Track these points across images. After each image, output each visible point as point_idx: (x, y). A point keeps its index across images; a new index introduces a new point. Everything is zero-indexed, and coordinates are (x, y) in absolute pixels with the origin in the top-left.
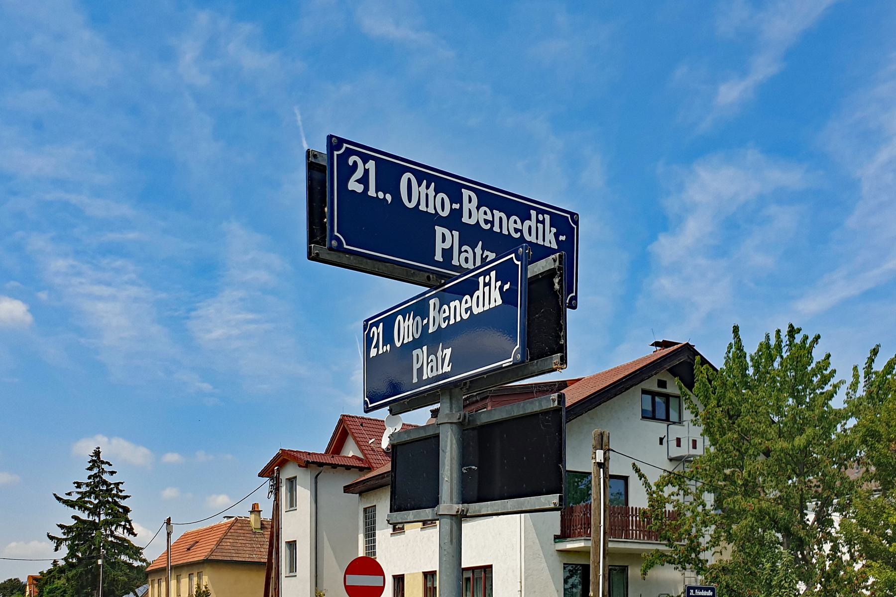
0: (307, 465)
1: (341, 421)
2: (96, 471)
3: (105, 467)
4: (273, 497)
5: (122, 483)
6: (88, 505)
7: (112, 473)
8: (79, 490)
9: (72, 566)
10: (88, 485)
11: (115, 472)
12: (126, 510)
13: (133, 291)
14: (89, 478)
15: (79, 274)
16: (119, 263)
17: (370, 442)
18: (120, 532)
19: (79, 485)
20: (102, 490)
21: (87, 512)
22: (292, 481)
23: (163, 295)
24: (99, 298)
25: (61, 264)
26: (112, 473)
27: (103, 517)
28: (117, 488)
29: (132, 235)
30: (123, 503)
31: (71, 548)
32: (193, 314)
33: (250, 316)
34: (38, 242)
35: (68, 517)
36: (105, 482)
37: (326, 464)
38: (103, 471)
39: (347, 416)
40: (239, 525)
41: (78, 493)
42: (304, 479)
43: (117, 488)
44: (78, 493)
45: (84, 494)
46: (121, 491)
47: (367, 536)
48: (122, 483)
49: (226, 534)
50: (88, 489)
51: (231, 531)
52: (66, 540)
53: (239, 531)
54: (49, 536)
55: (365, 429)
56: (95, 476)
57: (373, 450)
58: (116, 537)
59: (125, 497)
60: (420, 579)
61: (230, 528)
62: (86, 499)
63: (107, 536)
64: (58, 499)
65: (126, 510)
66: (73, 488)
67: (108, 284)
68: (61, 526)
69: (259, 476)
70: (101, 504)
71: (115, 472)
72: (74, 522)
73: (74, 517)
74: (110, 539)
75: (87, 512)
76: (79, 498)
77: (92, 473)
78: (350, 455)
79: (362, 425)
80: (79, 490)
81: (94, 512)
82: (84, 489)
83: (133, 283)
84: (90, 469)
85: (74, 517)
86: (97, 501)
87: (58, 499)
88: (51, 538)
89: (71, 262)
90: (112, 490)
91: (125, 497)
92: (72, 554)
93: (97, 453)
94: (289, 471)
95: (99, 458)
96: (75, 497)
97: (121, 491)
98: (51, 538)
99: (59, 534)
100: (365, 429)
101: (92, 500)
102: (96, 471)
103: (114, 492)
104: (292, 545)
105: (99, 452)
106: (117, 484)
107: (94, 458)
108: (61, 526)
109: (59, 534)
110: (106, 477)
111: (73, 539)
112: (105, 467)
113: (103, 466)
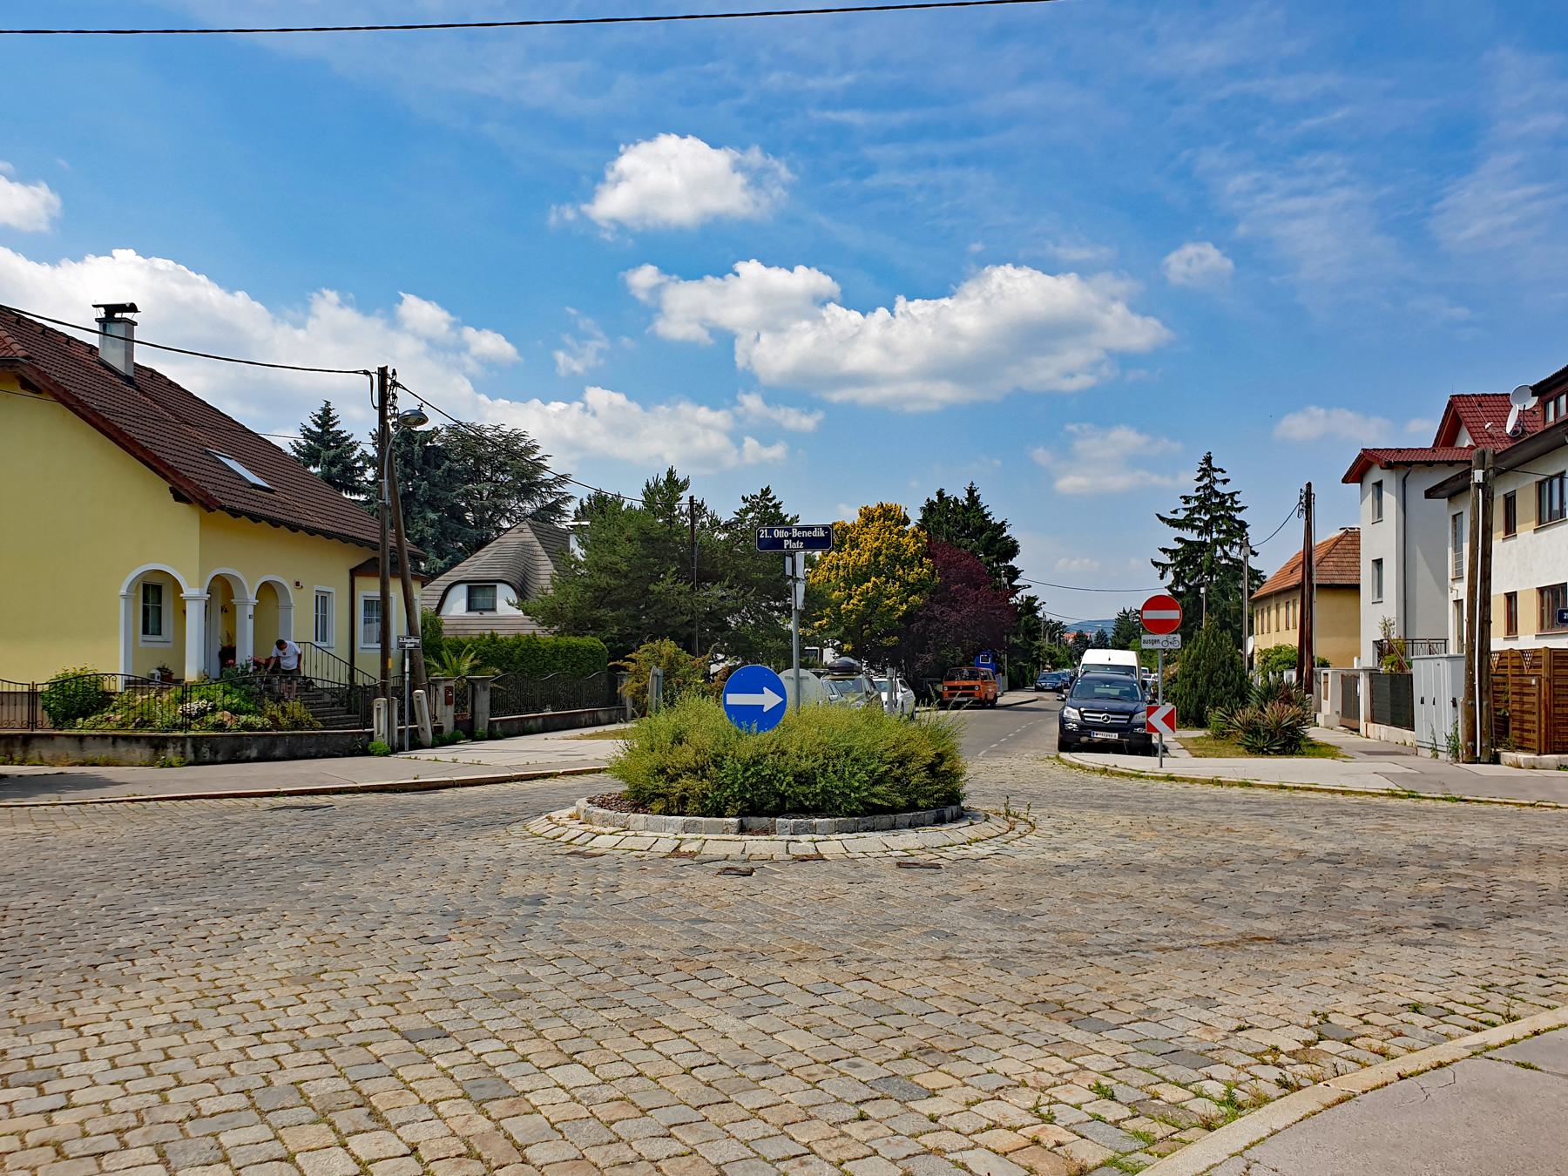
0: (1389, 466)
1: (1450, 404)
2: (1206, 481)
3: (1219, 476)
4: (1304, 516)
5: (1238, 493)
6: (1197, 523)
7: (1225, 481)
8: (1187, 506)
9: (1177, 595)
10: (1197, 498)
11: (1229, 480)
12: (1243, 525)
13: (1342, 194)
14: (1198, 490)
15: (1265, 189)
16: (1320, 159)
17: (1487, 426)
18: (1235, 553)
19: (1187, 500)
20: (1214, 504)
21: (1196, 532)
22: (1379, 485)
23: (1386, 190)
24: (1295, 215)
25: (1241, 182)
26: (1225, 481)
27: (1215, 535)
28: (1232, 499)
29: (1339, 114)
30: (1239, 516)
31: (1176, 574)
32: (1437, 206)
33: (1534, 189)
34: (1210, 159)
35: (1169, 537)
36: (1217, 494)
37: (1416, 462)
38: (1215, 481)
39: (1458, 396)
40: (1350, 539)
41: (1185, 509)
42: (1390, 480)
43: (1232, 499)
44: (1185, 509)
45: (1193, 510)
46: (1236, 503)
47: (1455, 550)
48: (1238, 493)
49: (1330, 552)
50: (1197, 504)
51: (1338, 547)
52: (1172, 565)
53: (1347, 547)
54: (1153, 562)
55: (1485, 409)
56: (1206, 487)
57: (1490, 436)
58: (1230, 559)
59: (1240, 509)
60: (1535, 597)
61: (1336, 544)
62: (1196, 516)
63: (1220, 558)
64: (1162, 519)
65: (1243, 525)
66: (1181, 504)
67: (1306, 192)
68: (1164, 550)
69: (1344, 481)
70: (1214, 519)
71: (1229, 480)
72: (1179, 546)
73: (1179, 540)
74: (1224, 562)
75: (1196, 532)
76: (1188, 516)
77: (1202, 484)
78: (1466, 446)
79: (1480, 405)
80: (1187, 506)
81: (1206, 529)
82: (1194, 504)
83: (1342, 183)
84: (1199, 479)
85: (1179, 540)
86: (1208, 516)
87: (1162, 519)
88: (1156, 564)
89: (1256, 175)
90: (1226, 501)
91: (1240, 509)
92: (1178, 579)
93: (1208, 460)
94: (1376, 474)
95: (1210, 465)
96: (1181, 515)
97: (1236, 503)
98: (1156, 564)
99: (1166, 559)
100: (1485, 409)
101: (1202, 517)
102: (1206, 481)
103: (1228, 504)
104: (1378, 563)
105: (1210, 458)
106: (1232, 495)
107: (1204, 466)
108: (1164, 550)
109: (1166, 559)
110: (1219, 487)
111: (1179, 564)
112: (1219, 476)
113: (1215, 474)
